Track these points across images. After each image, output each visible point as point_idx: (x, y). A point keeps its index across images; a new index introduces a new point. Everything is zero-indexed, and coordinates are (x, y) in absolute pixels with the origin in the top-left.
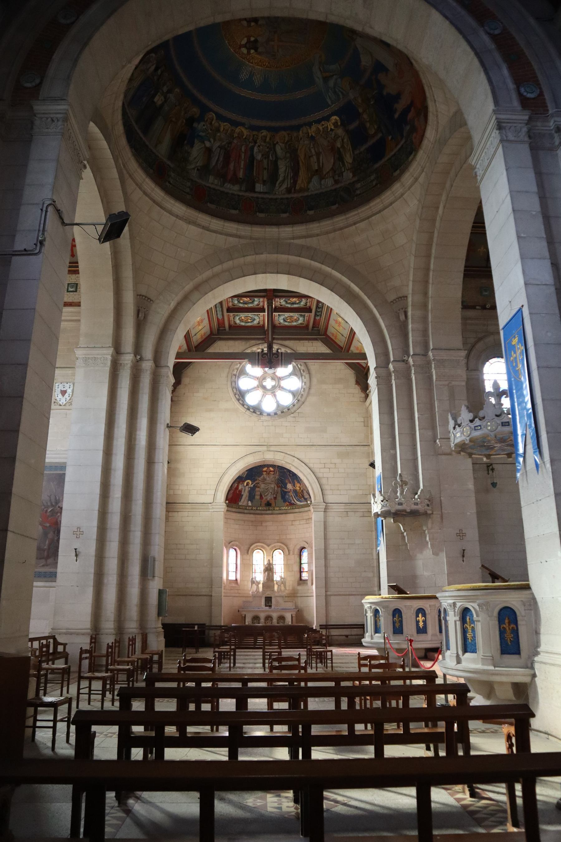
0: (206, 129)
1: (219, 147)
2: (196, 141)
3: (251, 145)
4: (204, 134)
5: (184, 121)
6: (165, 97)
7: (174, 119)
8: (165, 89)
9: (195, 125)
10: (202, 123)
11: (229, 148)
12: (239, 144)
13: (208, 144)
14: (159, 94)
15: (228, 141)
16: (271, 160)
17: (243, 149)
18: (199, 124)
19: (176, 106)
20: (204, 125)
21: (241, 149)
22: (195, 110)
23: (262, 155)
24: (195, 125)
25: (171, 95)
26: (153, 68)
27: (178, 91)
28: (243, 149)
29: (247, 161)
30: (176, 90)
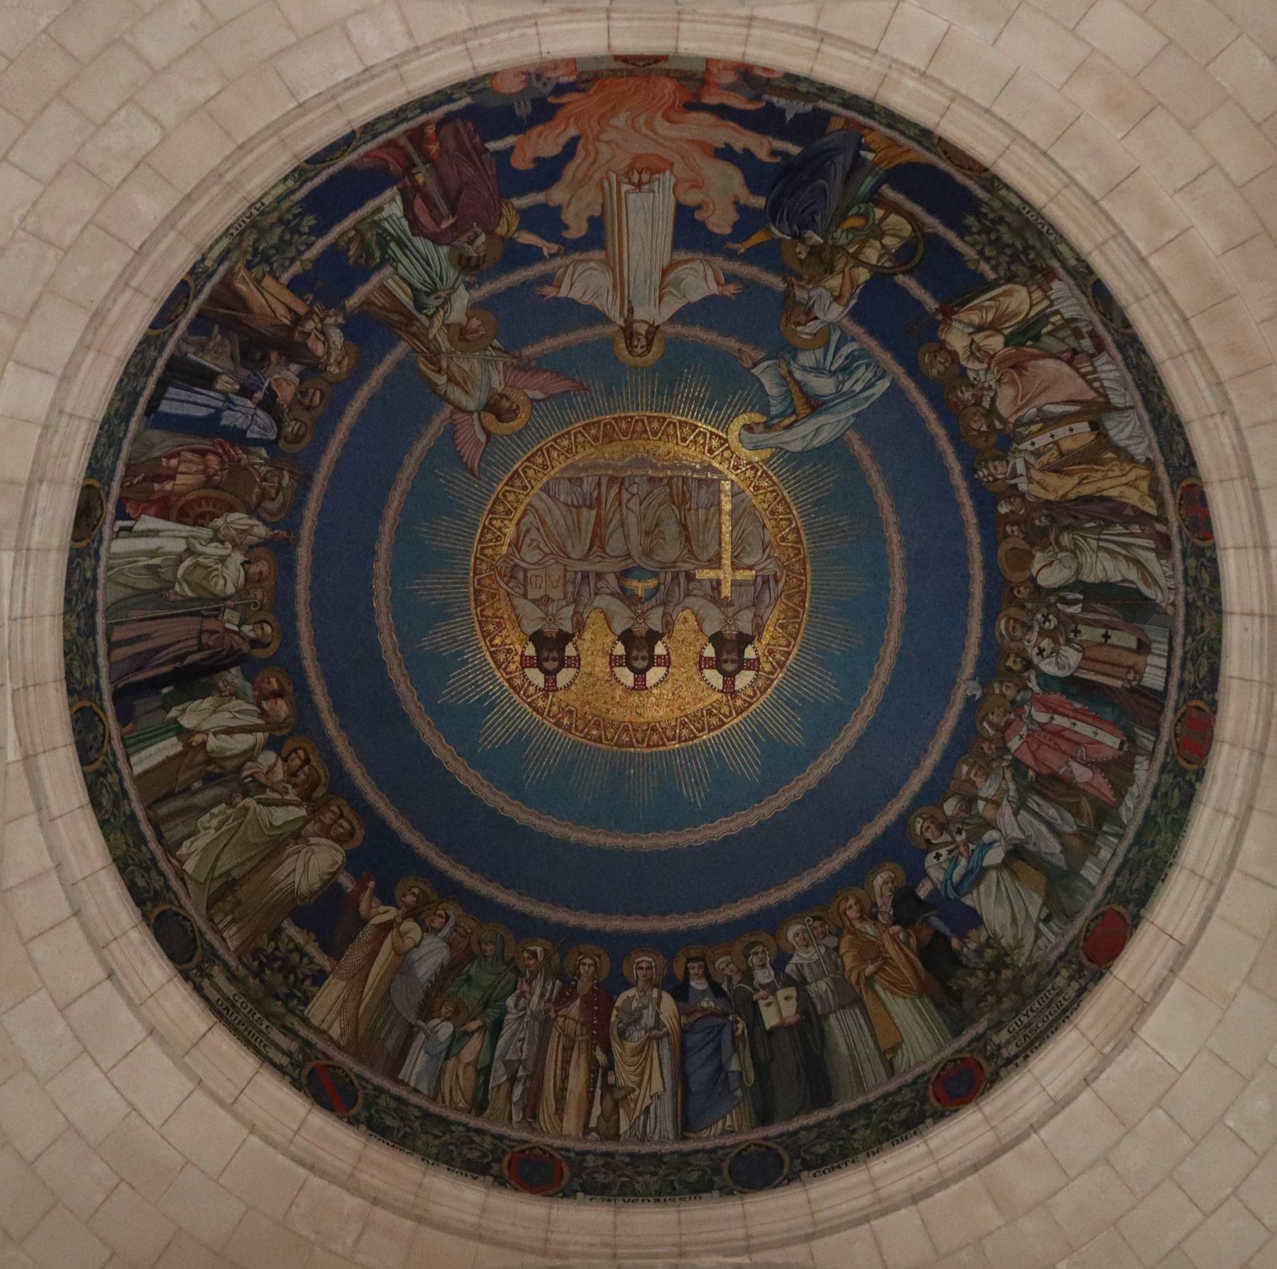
0: (950, 852)
1: (1016, 813)
2: (968, 901)
3: (1033, 685)
4: (963, 862)
5: (897, 928)
6: (789, 982)
7: (870, 969)
8: (764, 976)
9: (923, 891)
10: (930, 860)
11: (1031, 773)
12: (1024, 731)
13: (995, 856)
14: (761, 1003)
15: (1008, 775)
16: (1084, 609)
17: (1042, 717)
18: (925, 874)
19: (837, 949)
20: (938, 856)
21: (1041, 725)
22: (879, 880)
23: (1068, 642)
24: (923, 891)
25: (795, 959)
26: (668, 1003)
27: (799, 927)
28: (1042, 717)
29: (1078, 705)
30: (790, 936)
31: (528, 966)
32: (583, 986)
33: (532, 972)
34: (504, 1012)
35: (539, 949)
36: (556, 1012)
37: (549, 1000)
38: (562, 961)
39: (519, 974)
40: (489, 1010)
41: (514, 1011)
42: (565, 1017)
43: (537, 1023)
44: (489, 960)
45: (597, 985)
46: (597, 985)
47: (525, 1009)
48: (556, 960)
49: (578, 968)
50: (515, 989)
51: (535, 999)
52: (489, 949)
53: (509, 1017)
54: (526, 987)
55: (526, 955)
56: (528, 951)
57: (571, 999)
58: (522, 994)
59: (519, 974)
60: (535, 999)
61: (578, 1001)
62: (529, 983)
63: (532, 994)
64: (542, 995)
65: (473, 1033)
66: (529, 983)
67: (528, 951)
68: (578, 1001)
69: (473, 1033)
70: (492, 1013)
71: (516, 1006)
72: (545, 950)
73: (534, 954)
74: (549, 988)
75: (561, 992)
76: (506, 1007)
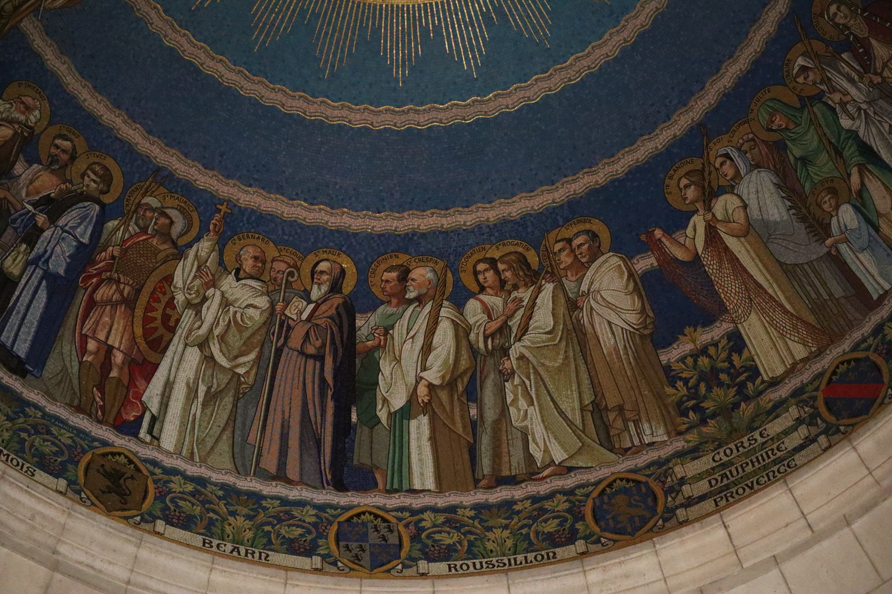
31: (815, 83)
32: (860, 28)
33: (821, 83)
34: (853, 135)
35: (801, 61)
36: (876, 74)
37: (861, 77)
38: (822, 40)
39: (819, 97)
40: (846, 153)
41: (858, 122)
42: (885, 65)
43: (881, 102)
44: (791, 126)
45: (864, 10)
46: (864, 10)
47: (860, 109)
48: (818, 46)
49: (837, 25)
50: (833, 110)
51: (853, 91)
52: (779, 121)
53: (861, 133)
54: (837, 97)
55: (801, 80)
56: (798, 75)
57: (868, 50)
58: (843, 104)
59: (819, 97)
60: (853, 91)
61: (873, 41)
62: (833, 90)
63: (846, 93)
64: (851, 81)
65: (862, 184)
66: (833, 90)
67: (798, 75)
68: (873, 41)
69: (862, 184)
70: (850, 151)
71: (853, 119)
72: (803, 55)
73: (804, 69)
74: (847, 69)
75: (857, 57)
76: (848, 131)
